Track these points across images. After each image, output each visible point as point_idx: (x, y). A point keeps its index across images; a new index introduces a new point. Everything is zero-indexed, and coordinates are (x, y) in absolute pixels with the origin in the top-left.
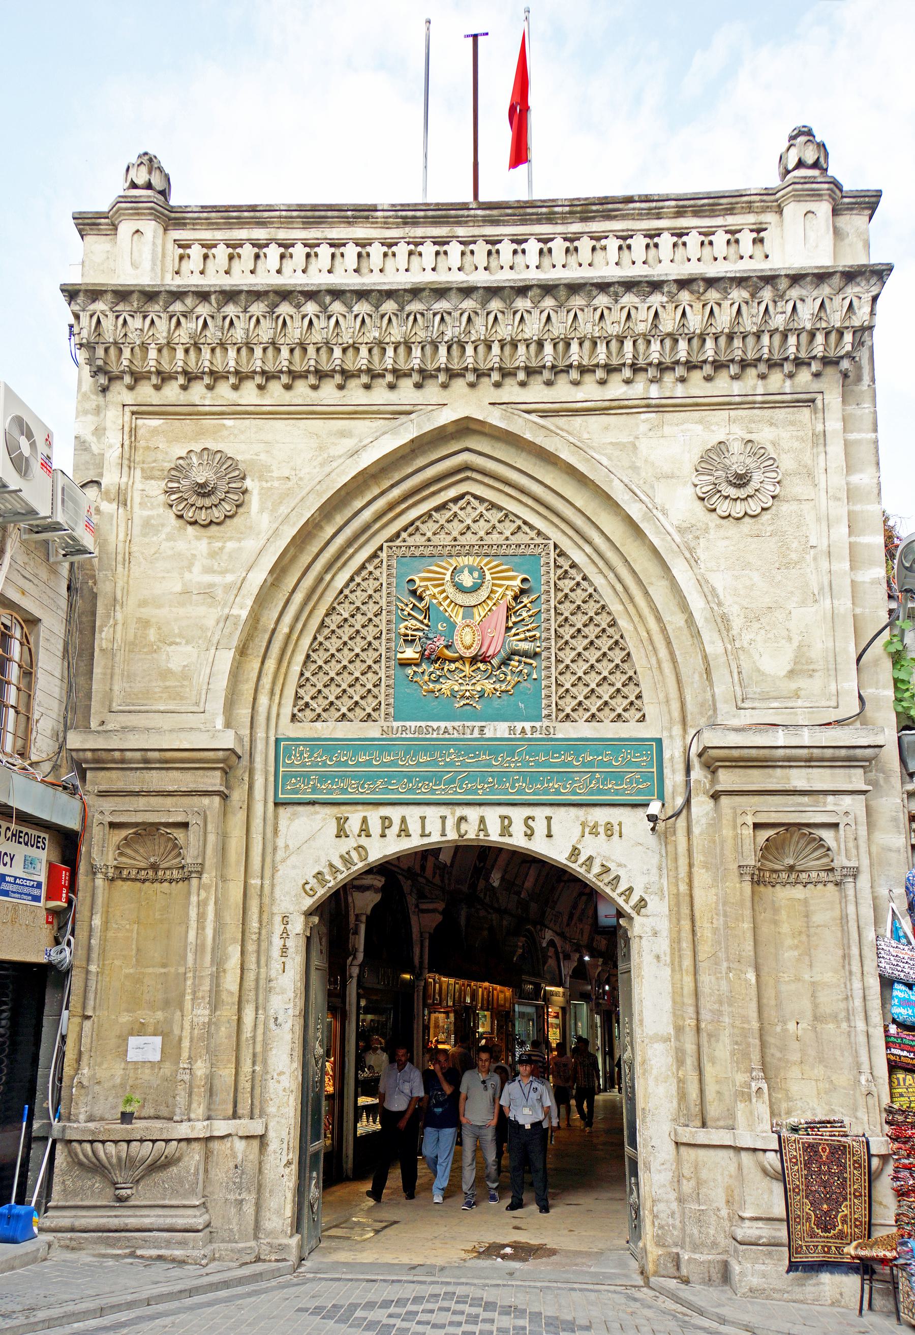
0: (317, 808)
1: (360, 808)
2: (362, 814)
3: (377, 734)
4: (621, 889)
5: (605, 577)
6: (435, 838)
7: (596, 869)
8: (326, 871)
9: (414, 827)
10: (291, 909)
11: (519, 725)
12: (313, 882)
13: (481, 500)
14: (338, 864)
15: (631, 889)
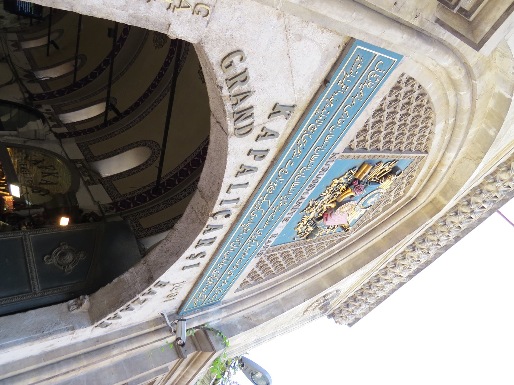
0: (317, 86)
1: (289, 130)
2: (280, 133)
3: (336, 151)
4: (121, 314)
5: (318, 260)
6: (222, 195)
7: (142, 298)
8: (245, 88)
9: (242, 179)
10: (215, 26)
11: (273, 240)
12: (239, 67)
13: (395, 202)
14: (245, 104)
15: (119, 318)
